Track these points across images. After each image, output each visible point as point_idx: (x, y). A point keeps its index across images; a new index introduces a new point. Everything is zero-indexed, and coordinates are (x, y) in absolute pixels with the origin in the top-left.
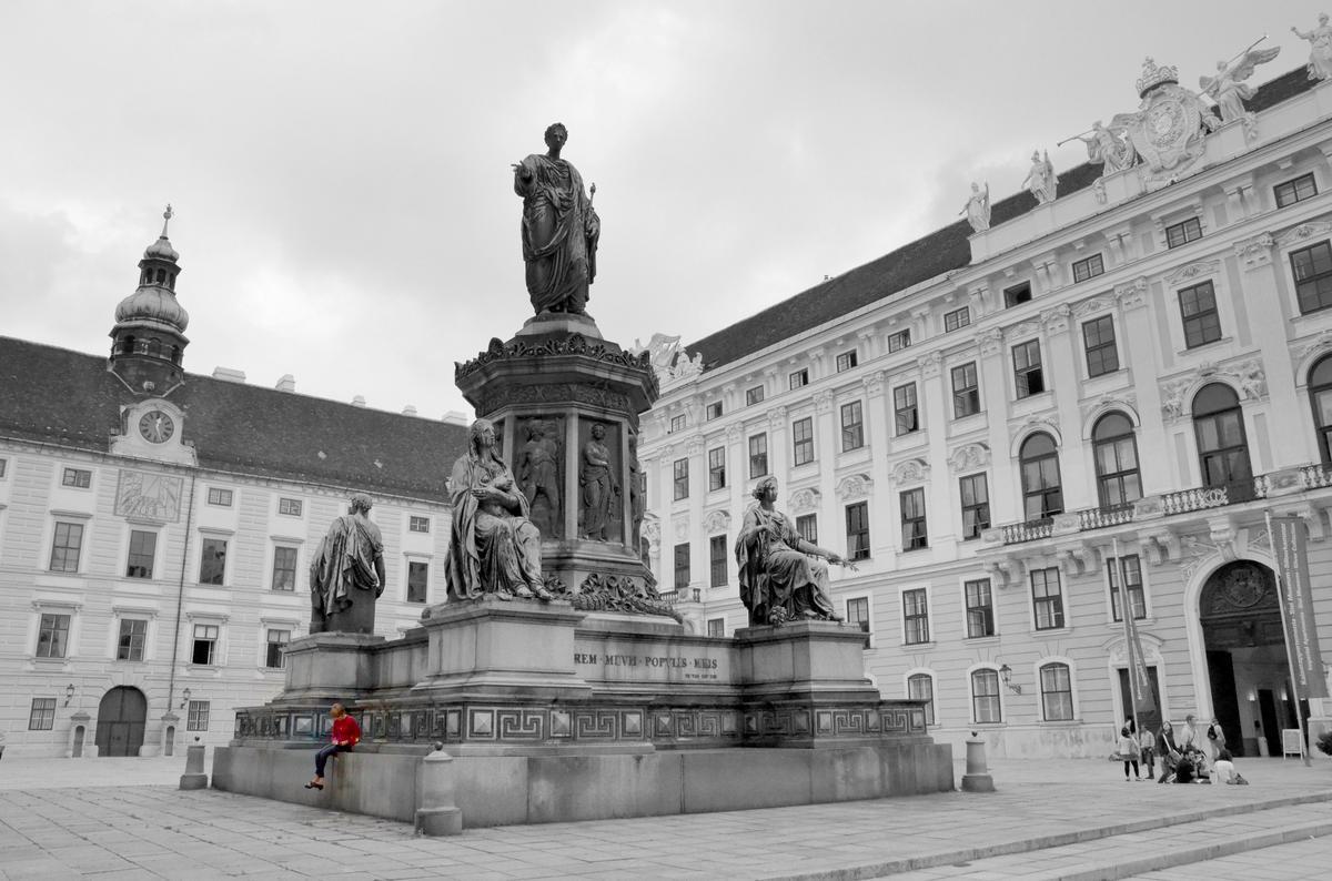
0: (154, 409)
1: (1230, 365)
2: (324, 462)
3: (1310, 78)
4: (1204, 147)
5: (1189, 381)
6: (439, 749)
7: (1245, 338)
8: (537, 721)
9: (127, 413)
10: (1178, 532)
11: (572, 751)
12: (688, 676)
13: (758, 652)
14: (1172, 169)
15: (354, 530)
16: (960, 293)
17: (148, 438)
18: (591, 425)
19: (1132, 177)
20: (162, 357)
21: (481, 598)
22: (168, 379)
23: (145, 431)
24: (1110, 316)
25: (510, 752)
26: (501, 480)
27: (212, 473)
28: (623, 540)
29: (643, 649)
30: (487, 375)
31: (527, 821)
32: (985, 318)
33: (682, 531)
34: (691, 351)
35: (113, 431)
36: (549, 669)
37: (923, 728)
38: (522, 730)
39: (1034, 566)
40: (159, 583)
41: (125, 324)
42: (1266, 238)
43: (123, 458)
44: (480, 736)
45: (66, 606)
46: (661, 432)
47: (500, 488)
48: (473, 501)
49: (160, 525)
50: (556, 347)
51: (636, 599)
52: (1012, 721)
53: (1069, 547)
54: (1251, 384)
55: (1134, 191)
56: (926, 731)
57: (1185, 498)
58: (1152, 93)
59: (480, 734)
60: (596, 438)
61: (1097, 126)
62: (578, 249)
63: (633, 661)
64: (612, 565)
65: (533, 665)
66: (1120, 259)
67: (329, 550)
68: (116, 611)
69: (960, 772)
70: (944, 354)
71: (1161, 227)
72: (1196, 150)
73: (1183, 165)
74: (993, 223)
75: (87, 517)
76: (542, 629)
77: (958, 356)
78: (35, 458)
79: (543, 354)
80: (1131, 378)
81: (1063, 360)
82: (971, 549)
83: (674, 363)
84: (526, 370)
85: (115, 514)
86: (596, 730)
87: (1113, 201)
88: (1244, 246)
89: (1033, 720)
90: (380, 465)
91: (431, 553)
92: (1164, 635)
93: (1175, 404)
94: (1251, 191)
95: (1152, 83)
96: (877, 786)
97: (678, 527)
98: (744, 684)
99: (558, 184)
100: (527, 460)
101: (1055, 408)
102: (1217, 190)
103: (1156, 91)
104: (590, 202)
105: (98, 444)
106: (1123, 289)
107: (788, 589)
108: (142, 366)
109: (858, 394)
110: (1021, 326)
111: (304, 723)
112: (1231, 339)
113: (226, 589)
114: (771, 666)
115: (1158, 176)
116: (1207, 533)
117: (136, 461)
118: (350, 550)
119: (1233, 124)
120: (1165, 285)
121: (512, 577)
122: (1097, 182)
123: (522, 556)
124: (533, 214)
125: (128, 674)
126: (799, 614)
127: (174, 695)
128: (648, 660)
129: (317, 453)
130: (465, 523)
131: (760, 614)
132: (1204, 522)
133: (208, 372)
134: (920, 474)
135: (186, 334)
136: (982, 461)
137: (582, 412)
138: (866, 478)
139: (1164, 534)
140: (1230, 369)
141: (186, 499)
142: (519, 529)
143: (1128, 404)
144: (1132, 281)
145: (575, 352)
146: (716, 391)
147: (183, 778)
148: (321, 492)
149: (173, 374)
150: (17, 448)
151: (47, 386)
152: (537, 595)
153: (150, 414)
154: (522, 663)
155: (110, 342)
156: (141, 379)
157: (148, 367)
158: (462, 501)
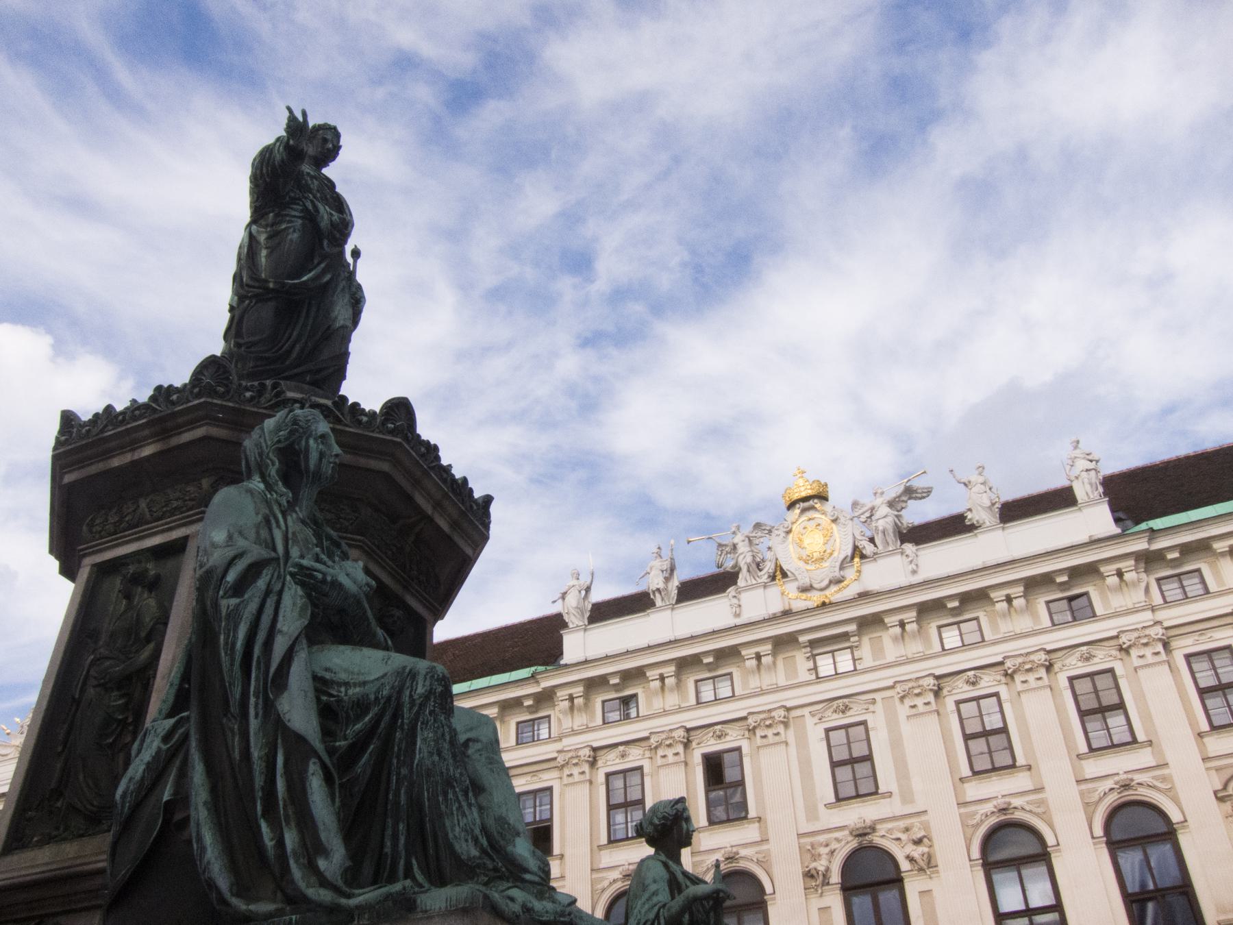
1: (890, 825)
4: (859, 571)
5: (838, 840)
7: (907, 797)
14: (822, 590)
16: (546, 697)
19: (774, 590)
24: (739, 749)
32: (574, 733)
42: (931, 681)
54: (917, 852)
55: (776, 607)
58: (802, 505)
72: (850, 573)
73: (834, 588)
77: (528, 778)
80: (764, 831)
87: (748, 615)
88: (907, 686)
93: (822, 869)
95: (804, 494)
110: (621, 748)
112: (890, 794)
115: (804, 596)
140: (890, 831)
143: (758, 862)
144: (770, 711)
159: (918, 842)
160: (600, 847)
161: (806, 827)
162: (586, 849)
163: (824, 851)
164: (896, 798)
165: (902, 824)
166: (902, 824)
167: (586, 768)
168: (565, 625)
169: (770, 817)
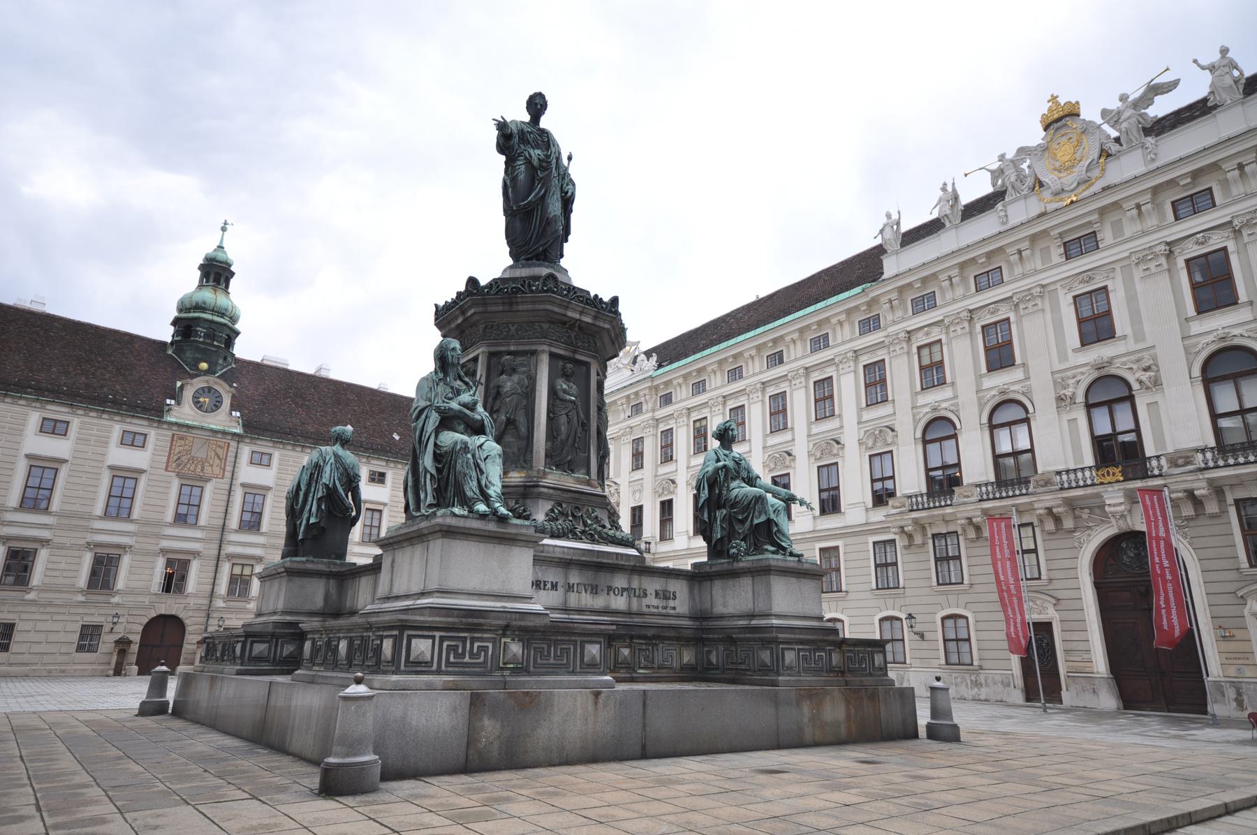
1: (1124, 359)
3: (1209, 104)
5: (1082, 373)
6: (358, 681)
7: (1139, 336)
8: (485, 649)
9: (182, 387)
10: (1071, 504)
11: (523, 684)
12: (648, 606)
13: (718, 586)
17: (200, 408)
18: (561, 363)
19: (1033, 200)
21: (434, 514)
22: (220, 361)
25: (451, 685)
26: (466, 397)
28: (588, 473)
29: (604, 579)
30: (463, 313)
31: (467, 768)
32: (894, 323)
33: (637, 495)
34: (648, 354)
35: (168, 401)
36: (504, 592)
37: (884, 670)
38: (467, 659)
39: (936, 531)
40: (202, 528)
43: (176, 424)
44: (418, 666)
45: (118, 546)
46: (622, 416)
47: (465, 405)
48: (434, 418)
49: (208, 480)
50: (530, 286)
51: (599, 529)
52: (916, 663)
53: (969, 515)
54: (1145, 376)
55: (1035, 212)
56: (886, 674)
57: (1080, 475)
58: (1056, 125)
59: (418, 663)
60: (567, 376)
61: (1002, 158)
62: (555, 207)
63: (594, 590)
64: (577, 496)
65: (486, 588)
66: (1018, 270)
67: (306, 478)
68: (164, 551)
69: (923, 717)
70: (857, 353)
71: (1059, 242)
72: (1096, 173)
73: (1083, 187)
74: (903, 244)
76: (498, 549)
78: (95, 421)
79: (516, 293)
81: (964, 356)
82: (879, 515)
83: (634, 362)
84: (500, 308)
85: (166, 470)
86: (552, 661)
87: (1013, 221)
89: (935, 663)
90: (397, 437)
92: (1059, 594)
94: (1149, 206)
95: (1056, 116)
96: (843, 730)
97: (634, 492)
98: (701, 616)
99: (537, 146)
100: (498, 393)
101: (956, 397)
102: (1116, 205)
103: (1060, 124)
104: (567, 169)
105: (155, 412)
106: (1020, 296)
107: (748, 523)
108: (198, 349)
109: (784, 387)
111: (260, 648)
112: (1125, 337)
113: (262, 534)
114: (733, 600)
116: (1102, 507)
117: (188, 427)
118: (325, 479)
119: (1132, 148)
120: (1061, 292)
121: (469, 494)
122: (999, 206)
123: (482, 472)
124: (513, 172)
125: (170, 605)
126: (758, 549)
127: (212, 621)
128: (610, 589)
130: (424, 439)
131: (719, 548)
132: (1098, 495)
133: (256, 358)
134: (835, 451)
135: (238, 326)
136: (889, 440)
137: (553, 350)
138: (790, 454)
139: (1059, 506)
140: (1124, 364)
141: (231, 459)
142: (481, 446)
143: (1023, 394)
145: (546, 291)
146: (667, 384)
147: (143, 703)
149: (225, 359)
152: (495, 512)
153: (203, 389)
154: (473, 583)
155: (172, 329)
157: (204, 351)
158: (423, 416)
159: (1146, 369)
160: (917, 394)
161: (1057, 367)
162: (908, 395)
163: (1071, 381)
164: (1131, 340)
165: (1133, 358)
166: (1133, 358)
167: (904, 345)
168: (885, 252)
169: (1031, 363)
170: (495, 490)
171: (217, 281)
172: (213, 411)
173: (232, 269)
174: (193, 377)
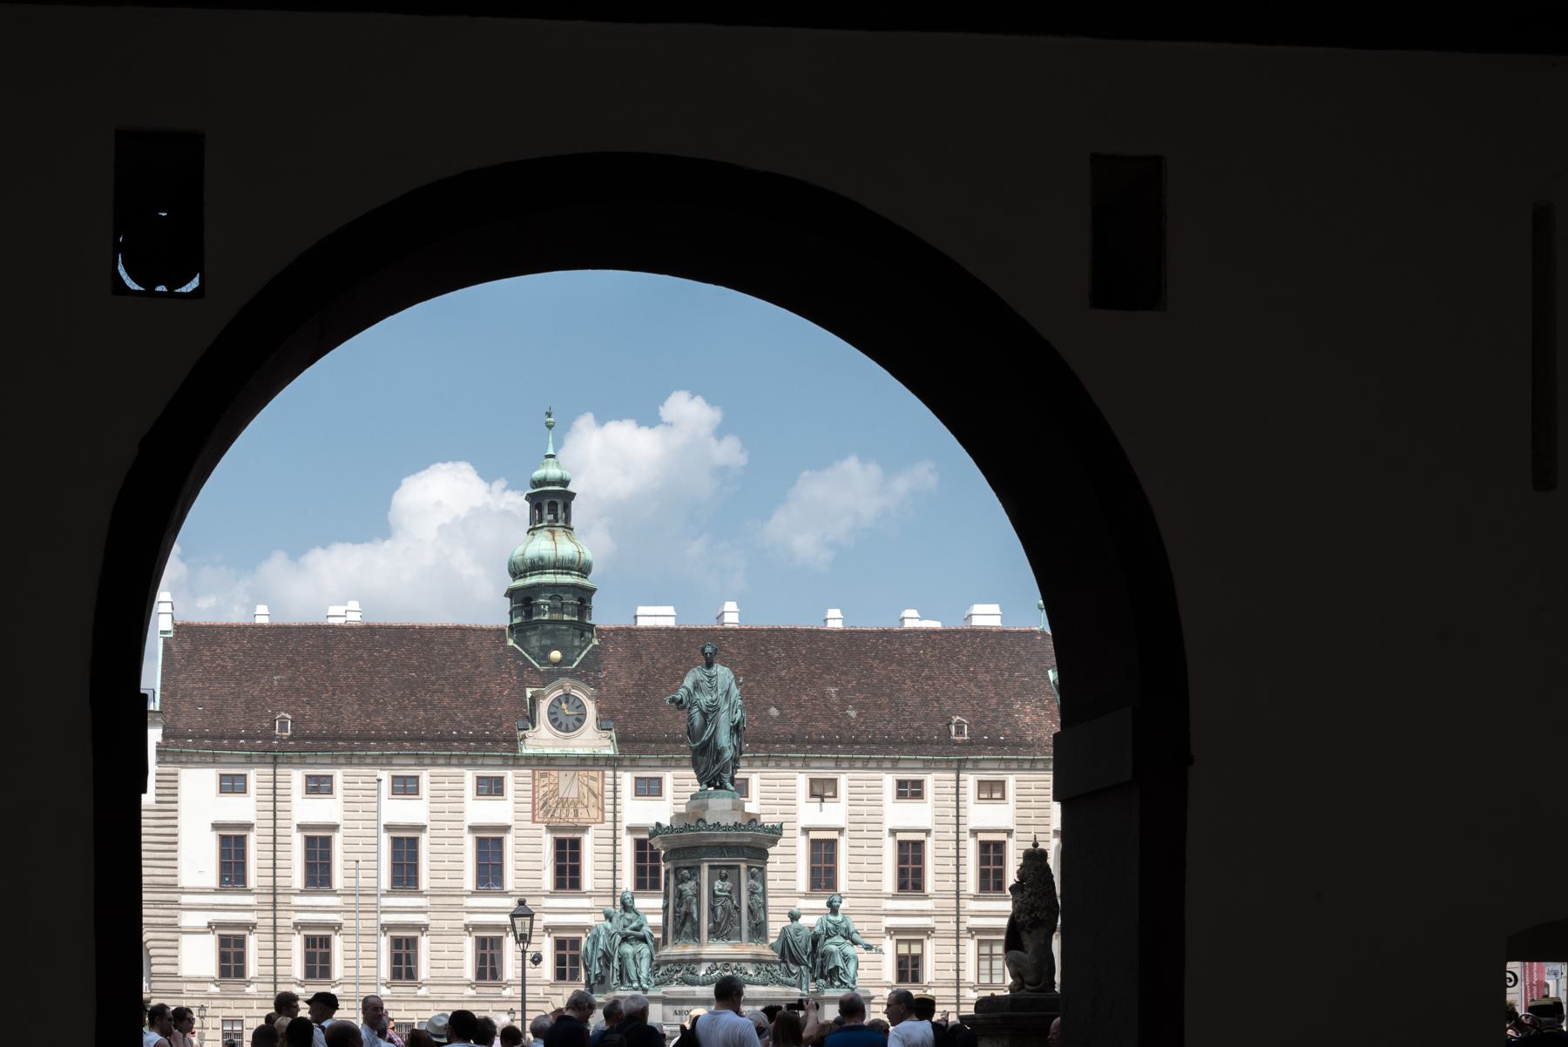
0: (560, 692)
2: (777, 721)
15: (603, 932)
17: (559, 728)
20: (566, 618)
22: (577, 643)
23: (555, 721)
26: (634, 924)
27: (633, 760)
35: (521, 724)
41: (520, 583)
43: (534, 756)
48: (619, 938)
60: (724, 879)
75: (506, 829)
78: (445, 770)
85: (534, 821)
90: (853, 714)
91: (927, 825)
108: (545, 634)
129: (766, 709)
148: (772, 764)
150: (427, 761)
151: (446, 679)
153: (558, 699)
156: (546, 650)
157: (552, 634)
170: (644, 975)
171: (553, 508)
172: (576, 728)
173: (570, 488)
174: (547, 679)
